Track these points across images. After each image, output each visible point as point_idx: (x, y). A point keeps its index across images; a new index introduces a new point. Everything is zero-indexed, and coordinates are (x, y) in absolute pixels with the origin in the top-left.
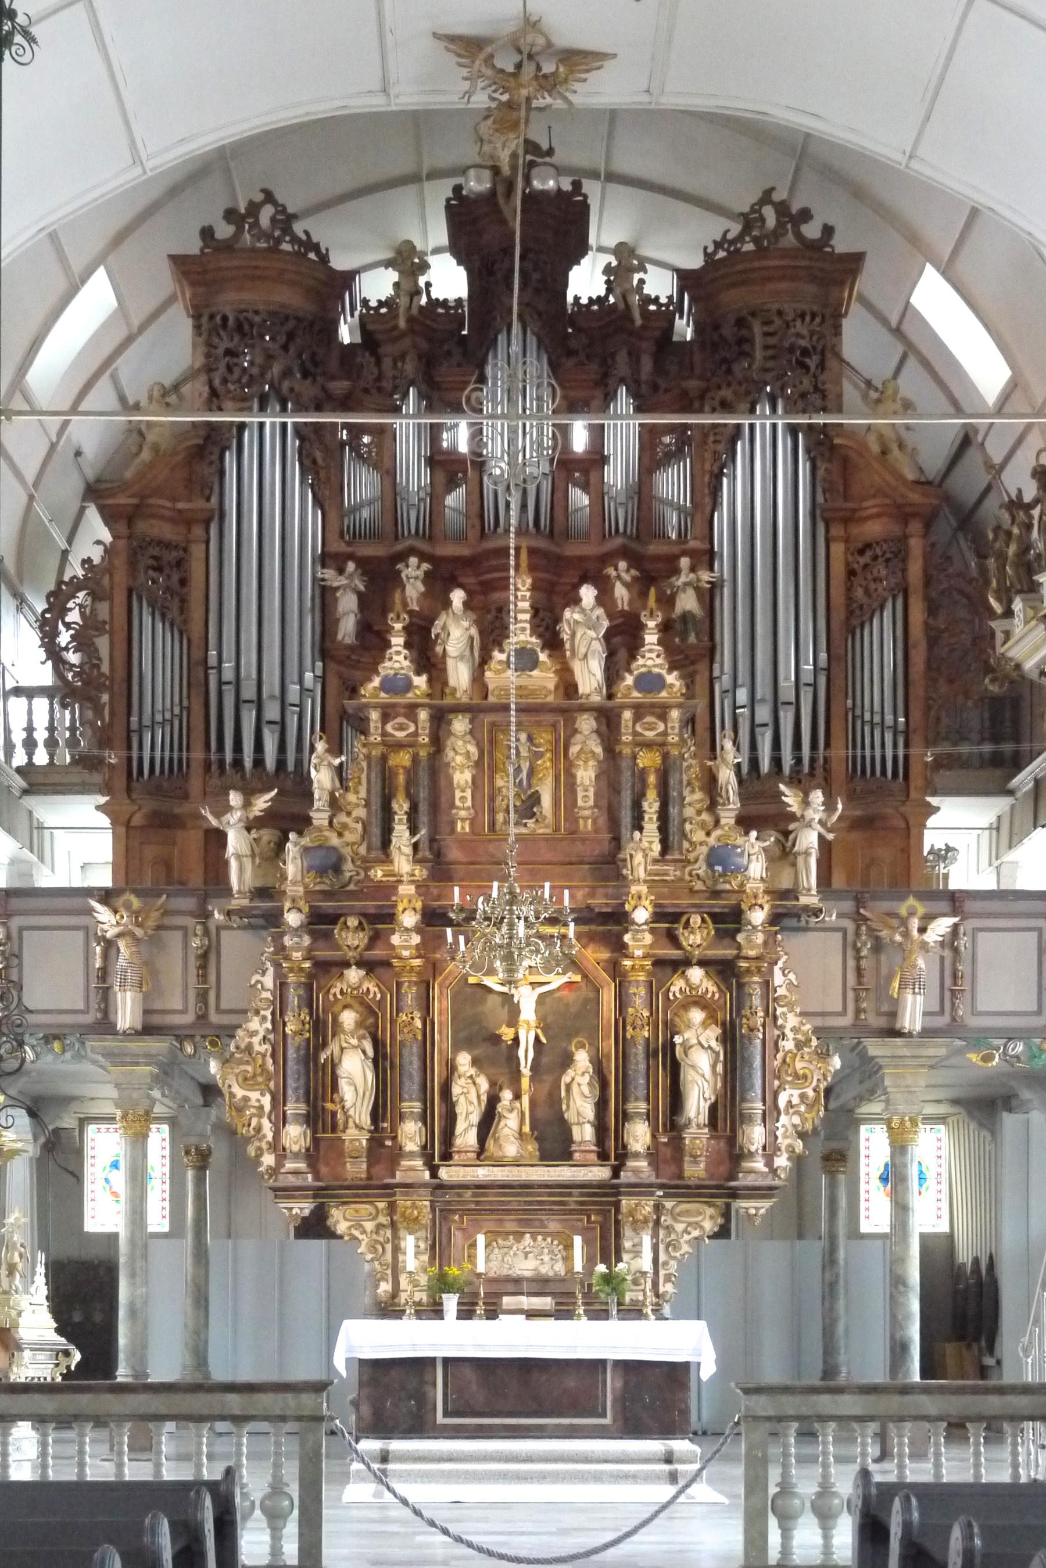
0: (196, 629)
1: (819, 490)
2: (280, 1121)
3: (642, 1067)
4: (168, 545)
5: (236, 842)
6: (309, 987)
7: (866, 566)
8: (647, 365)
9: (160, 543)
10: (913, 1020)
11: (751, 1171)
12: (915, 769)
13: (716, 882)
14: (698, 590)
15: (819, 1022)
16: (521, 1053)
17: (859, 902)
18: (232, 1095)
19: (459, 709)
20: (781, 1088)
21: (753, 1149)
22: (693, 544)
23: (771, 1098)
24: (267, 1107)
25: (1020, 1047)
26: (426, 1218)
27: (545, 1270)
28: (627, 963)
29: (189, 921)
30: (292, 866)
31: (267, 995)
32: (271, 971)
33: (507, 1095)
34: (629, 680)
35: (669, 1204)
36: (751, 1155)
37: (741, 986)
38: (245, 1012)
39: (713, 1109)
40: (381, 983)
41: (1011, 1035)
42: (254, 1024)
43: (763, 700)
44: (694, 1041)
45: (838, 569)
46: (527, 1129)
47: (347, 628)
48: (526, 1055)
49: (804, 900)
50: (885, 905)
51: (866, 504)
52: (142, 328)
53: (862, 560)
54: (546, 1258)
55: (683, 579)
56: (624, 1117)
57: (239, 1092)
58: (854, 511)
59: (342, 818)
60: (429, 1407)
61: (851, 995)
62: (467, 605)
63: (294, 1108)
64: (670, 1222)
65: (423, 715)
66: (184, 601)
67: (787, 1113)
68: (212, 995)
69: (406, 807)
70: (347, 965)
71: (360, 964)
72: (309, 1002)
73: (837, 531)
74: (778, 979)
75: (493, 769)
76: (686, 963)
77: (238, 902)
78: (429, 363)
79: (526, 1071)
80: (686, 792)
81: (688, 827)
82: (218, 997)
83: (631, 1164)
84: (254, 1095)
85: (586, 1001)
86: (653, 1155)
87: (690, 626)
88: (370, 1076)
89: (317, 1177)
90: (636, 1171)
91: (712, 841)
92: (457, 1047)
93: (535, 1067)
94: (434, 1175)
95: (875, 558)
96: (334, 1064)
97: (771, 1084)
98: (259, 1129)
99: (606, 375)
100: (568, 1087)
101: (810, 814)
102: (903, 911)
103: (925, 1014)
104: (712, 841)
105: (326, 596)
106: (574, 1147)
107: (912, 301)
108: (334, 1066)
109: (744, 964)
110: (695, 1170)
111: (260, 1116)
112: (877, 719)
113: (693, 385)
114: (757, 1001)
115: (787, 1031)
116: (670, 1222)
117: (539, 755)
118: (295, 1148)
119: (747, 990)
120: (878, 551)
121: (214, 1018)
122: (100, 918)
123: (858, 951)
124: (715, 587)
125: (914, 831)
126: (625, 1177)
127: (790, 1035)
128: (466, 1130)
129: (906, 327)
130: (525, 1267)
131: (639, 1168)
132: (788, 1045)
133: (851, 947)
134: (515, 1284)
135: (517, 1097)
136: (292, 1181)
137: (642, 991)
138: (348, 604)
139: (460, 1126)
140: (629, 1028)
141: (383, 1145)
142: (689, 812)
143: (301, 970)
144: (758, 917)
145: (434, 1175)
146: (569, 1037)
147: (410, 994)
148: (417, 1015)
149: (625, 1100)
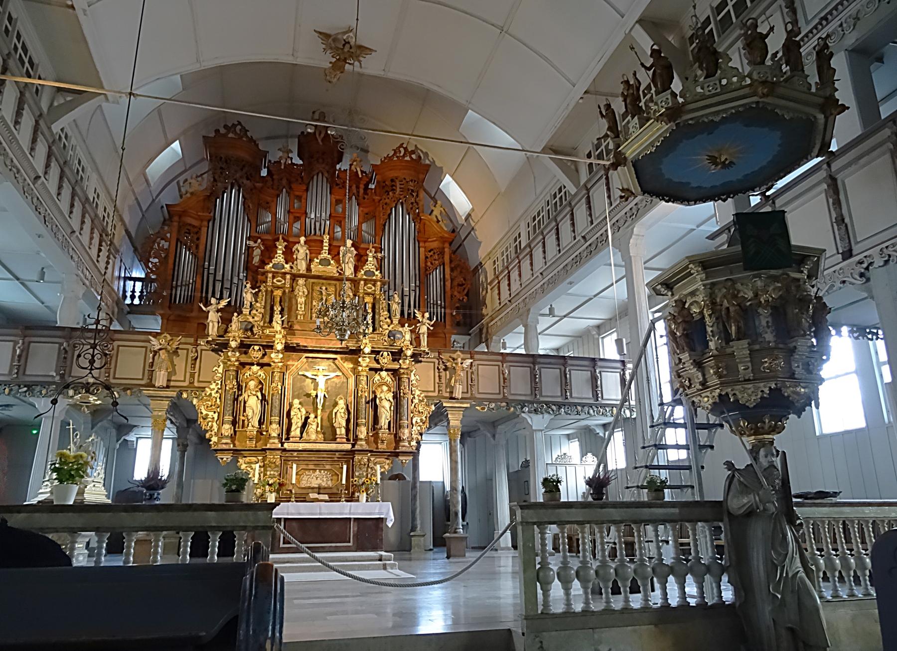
0: (201, 254)
3: (364, 406)
4: (194, 226)
6: (237, 372)
7: (431, 256)
9: (190, 225)
10: (458, 394)
15: (426, 394)
16: (318, 400)
18: (202, 413)
19: (302, 276)
24: (216, 418)
25: (494, 405)
26: (278, 462)
27: (324, 484)
28: (360, 368)
29: (190, 347)
30: (234, 325)
31: (220, 375)
32: (222, 366)
33: (312, 416)
34: (363, 272)
35: (372, 459)
37: (400, 379)
38: (210, 382)
40: (265, 372)
41: (490, 401)
42: (213, 386)
44: (383, 398)
45: (422, 257)
46: (319, 429)
48: (320, 402)
52: (190, 168)
54: (325, 479)
56: (357, 425)
57: (204, 412)
59: (254, 312)
60: (277, 540)
61: (437, 385)
62: (305, 243)
63: (229, 418)
64: (373, 466)
65: (288, 277)
66: (197, 247)
68: (196, 375)
69: (279, 309)
70: (253, 364)
71: (258, 364)
74: (413, 378)
75: (312, 299)
76: (381, 370)
77: (210, 339)
79: (320, 407)
80: (381, 311)
81: (381, 323)
82: (199, 375)
83: (359, 443)
84: (211, 414)
85: (343, 382)
86: (367, 441)
88: (259, 406)
89: (234, 445)
90: (361, 445)
91: (390, 328)
92: (293, 398)
93: (323, 406)
94: (282, 445)
95: (434, 253)
98: (212, 426)
100: (336, 413)
101: (424, 320)
104: (390, 328)
106: (337, 436)
108: (245, 403)
109: (402, 371)
111: (213, 422)
116: (373, 466)
117: (330, 295)
118: (226, 434)
119: (403, 380)
121: (196, 384)
122: (153, 343)
124: (383, 258)
126: (357, 447)
128: (296, 429)
131: (362, 445)
136: (225, 447)
137: (365, 379)
138: (257, 252)
139: (293, 428)
140: (360, 392)
141: (262, 435)
142: (382, 318)
143: (234, 365)
145: (282, 445)
147: (277, 376)
148: (279, 384)
149: (357, 419)
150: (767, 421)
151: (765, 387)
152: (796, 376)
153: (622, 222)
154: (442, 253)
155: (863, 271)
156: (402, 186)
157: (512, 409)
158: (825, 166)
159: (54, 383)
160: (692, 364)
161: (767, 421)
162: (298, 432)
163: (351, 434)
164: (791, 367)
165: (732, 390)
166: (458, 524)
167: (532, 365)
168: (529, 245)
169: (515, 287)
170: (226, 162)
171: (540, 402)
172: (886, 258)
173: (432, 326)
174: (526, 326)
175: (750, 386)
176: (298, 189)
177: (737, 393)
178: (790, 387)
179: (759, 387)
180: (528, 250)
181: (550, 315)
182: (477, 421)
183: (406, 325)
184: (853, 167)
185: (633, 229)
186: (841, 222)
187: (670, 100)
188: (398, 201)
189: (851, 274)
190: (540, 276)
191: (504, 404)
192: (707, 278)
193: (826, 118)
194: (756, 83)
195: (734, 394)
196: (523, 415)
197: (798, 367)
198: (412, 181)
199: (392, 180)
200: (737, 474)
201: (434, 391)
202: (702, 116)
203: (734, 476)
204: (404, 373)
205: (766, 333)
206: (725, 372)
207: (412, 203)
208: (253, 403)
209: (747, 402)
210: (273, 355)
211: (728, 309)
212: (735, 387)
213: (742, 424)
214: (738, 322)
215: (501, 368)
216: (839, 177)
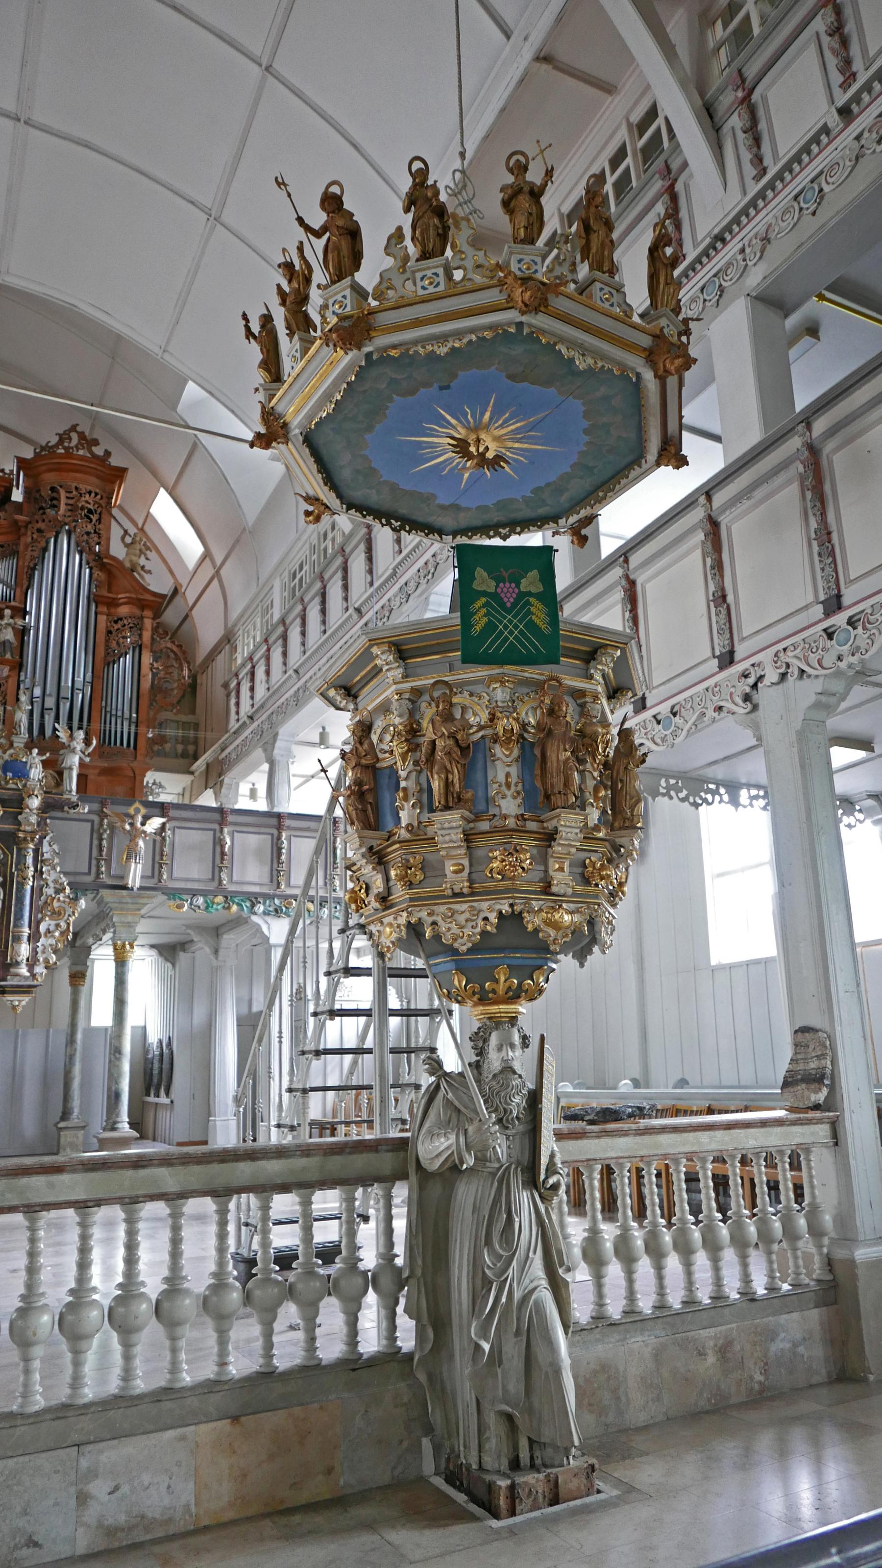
1: (93, 586)
11: (17, 975)
12: (142, 743)
13: (7, 783)
14: (13, 628)
15: (72, 879)
17: (103, 804)
20: (42, 919)
21: (19, 959)
22: (13, 603)
23: (35, 925)
25: (201, 900)
36: (17, 964)
41: (194, 893)
43: (50, 695)
50: (121, 809)
51: (120, 596)
53: (116, 627)
55: (5, 621)
58: (114, 599)
61: (94, 862)
67: (46, 936)
73: (104, 609)
74: (46, 848)
87: (7, 648)
97: (36, 916)
102: (132, 811)
103: (142, 877)
107: (151, 511)
112: (119, 713)
114: (30, 860)
115: (50, 882)
120: (126, 622)
123: (101, 835)
125: (138, 778)
127: (51, 885)
129: (146, 528)
132: (50, 891)
133: (96, 833)
144: (35, 803)
150: (502, 979)
151: (490, 909)
152: (554, 889)
153: (412, 585)
154: (138, 627)
155: (748, 690)
156: (71, 502)
157: (235, 908)
158: (702, 500)
160: (363, 856)
161: (502, 979)
164: (546, 871)
165: (429, 914)
166: (118, 1115)
168: (283, 621)
169: (261, 692)
171: (286, 897)
172: (782, 670)
173: (89, 755)
174: (272, 763)
175: (465, 907)
177: (439, 919)
178: (540, 910)
179: (480, 911)
180: (281, 629)
181: (321, 744)
182: (188, 927)
183: (35, 751)
184: (747, 504)
185: (427, 599)
186: (720, 600)
187: (348, 301)
188: (62, 527)
189: (731, 694)
190: (294, 676)
191: (220, 899)
192: (406, 676)
193: (662, 379)
194: (510, 280)
195: (434, 923)
196: (254, 918)
197: (561, 869)
198: (90, 493)
199: (53, 489)
200: (443, 1084)
201: (89, 873)
202: (415, 342)
203: (438, 1087)
204: (25, 839)
205: (504, 797)
206: (420, 876)
207: (88, 533)
209: (455, 940)
211: (433, 743)
212: (435, 908)
213: (456, 982)
214: (448, 772)
215: (218, 834)
216: (724, 520)
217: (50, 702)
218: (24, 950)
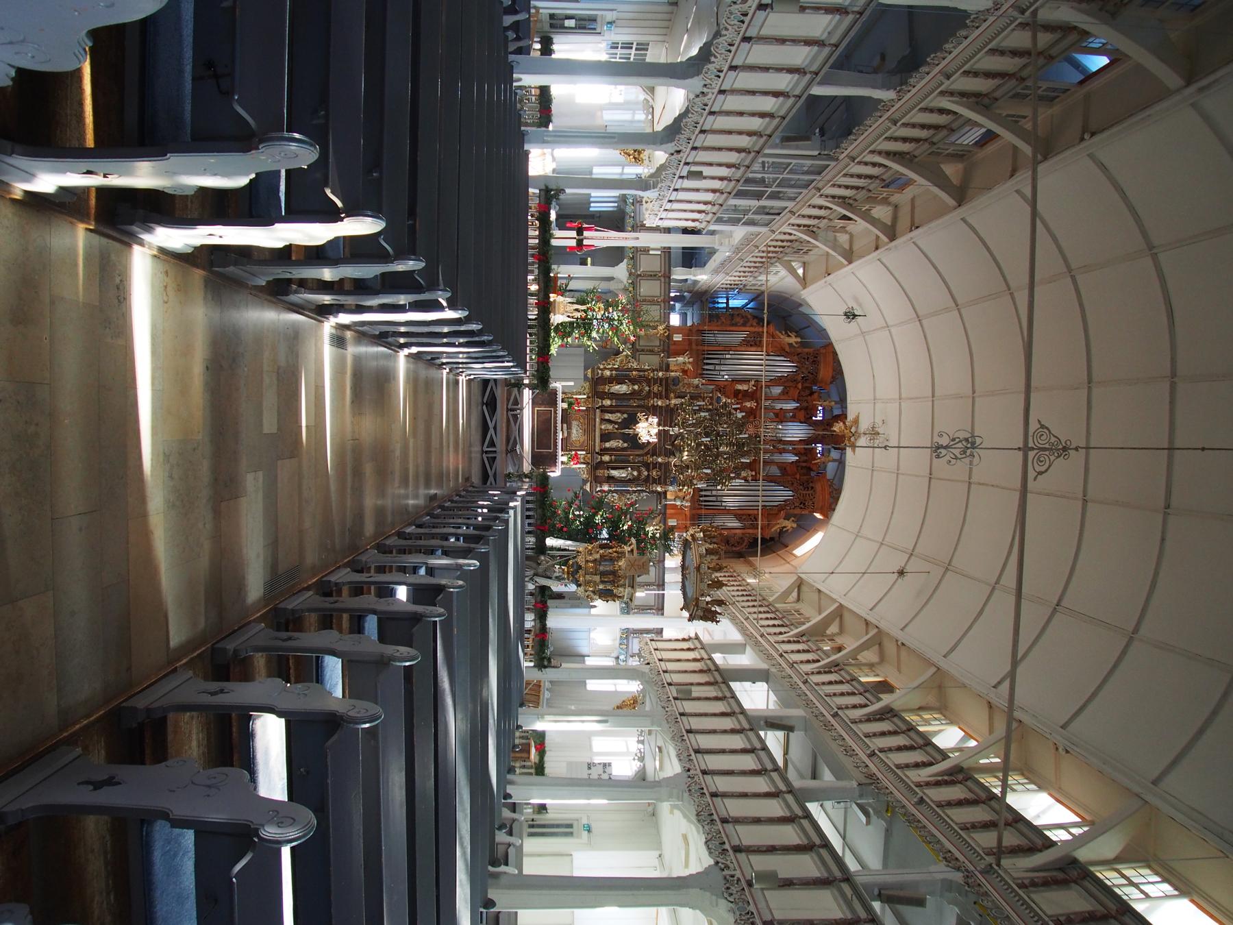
0: (738, 349)
2: (611, 370)
5: (680, 359)
8: (804, 464)
33: (616, 426)
39: (613, 477)
42: (635, 364)
45: (751, 512)
47: (739, 387)
48: (626, 431)
49: (663, 500)
72: (640, 376)
78: (806, 409)
96: (625, 383)
99: (801, 454)
105: (746, 381)
110: (600, 473)
113: (798, 477)
130: (574, 431)
132: (628, 496)
134: (569, 428)
135: (617, 429)
136: (596, 373)
139: (610, 415)
144: (659, 489)
146: (632, 443)
147: (642, 403)
159: (636, 271)
162: (607, 418)
163: (604, 451)
167: (657, 583)
170: (814, 361)
176: (801, 414)
208: (622, 389)
210: (655, 399)
217: (714, 493)
218: (606, 488)
